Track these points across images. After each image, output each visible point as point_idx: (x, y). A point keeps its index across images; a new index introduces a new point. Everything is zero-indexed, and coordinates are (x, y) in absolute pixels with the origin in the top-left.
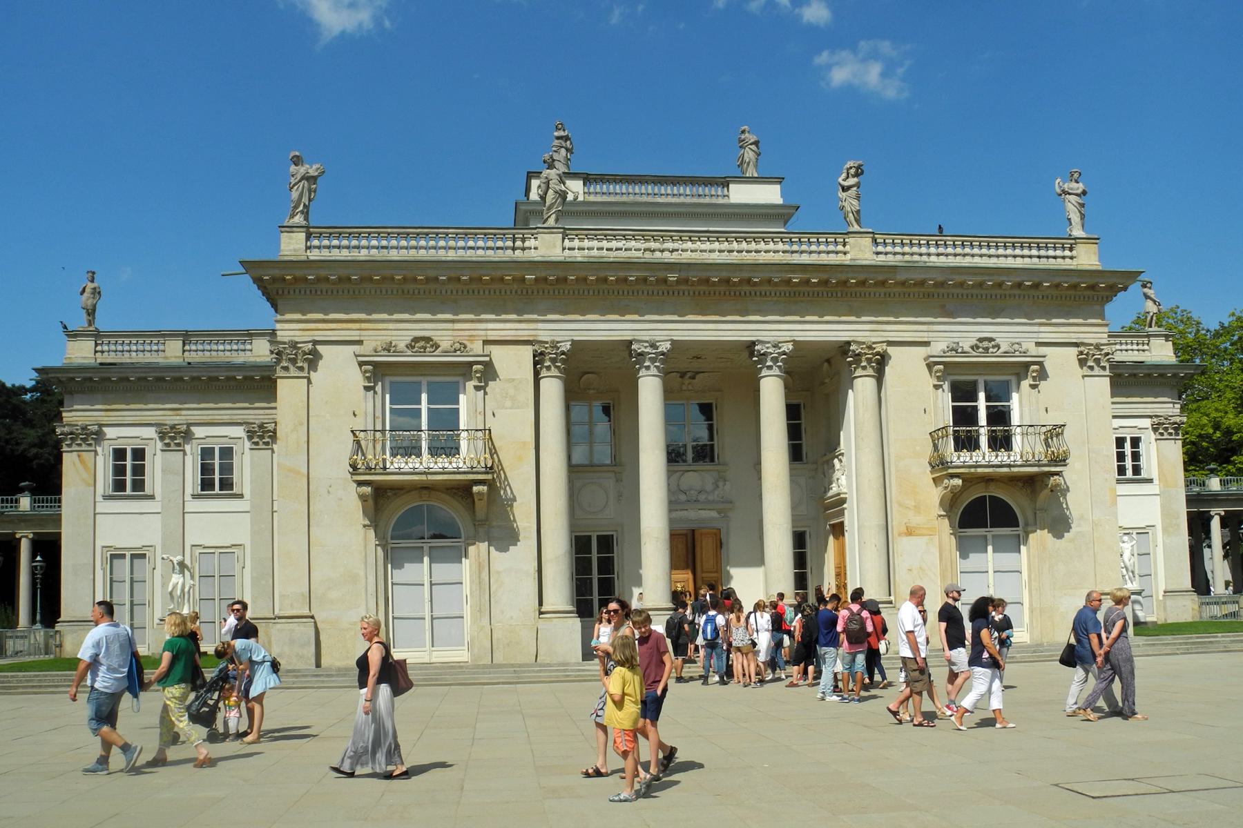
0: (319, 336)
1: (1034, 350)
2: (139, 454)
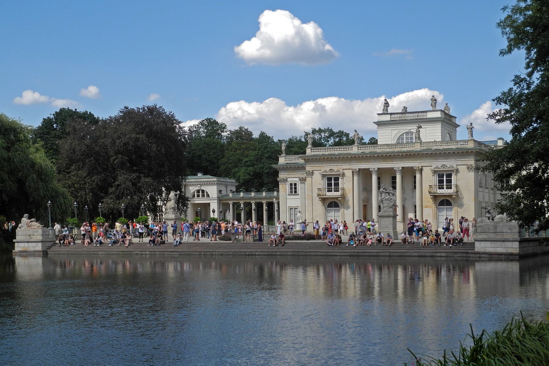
2: (295, 184)
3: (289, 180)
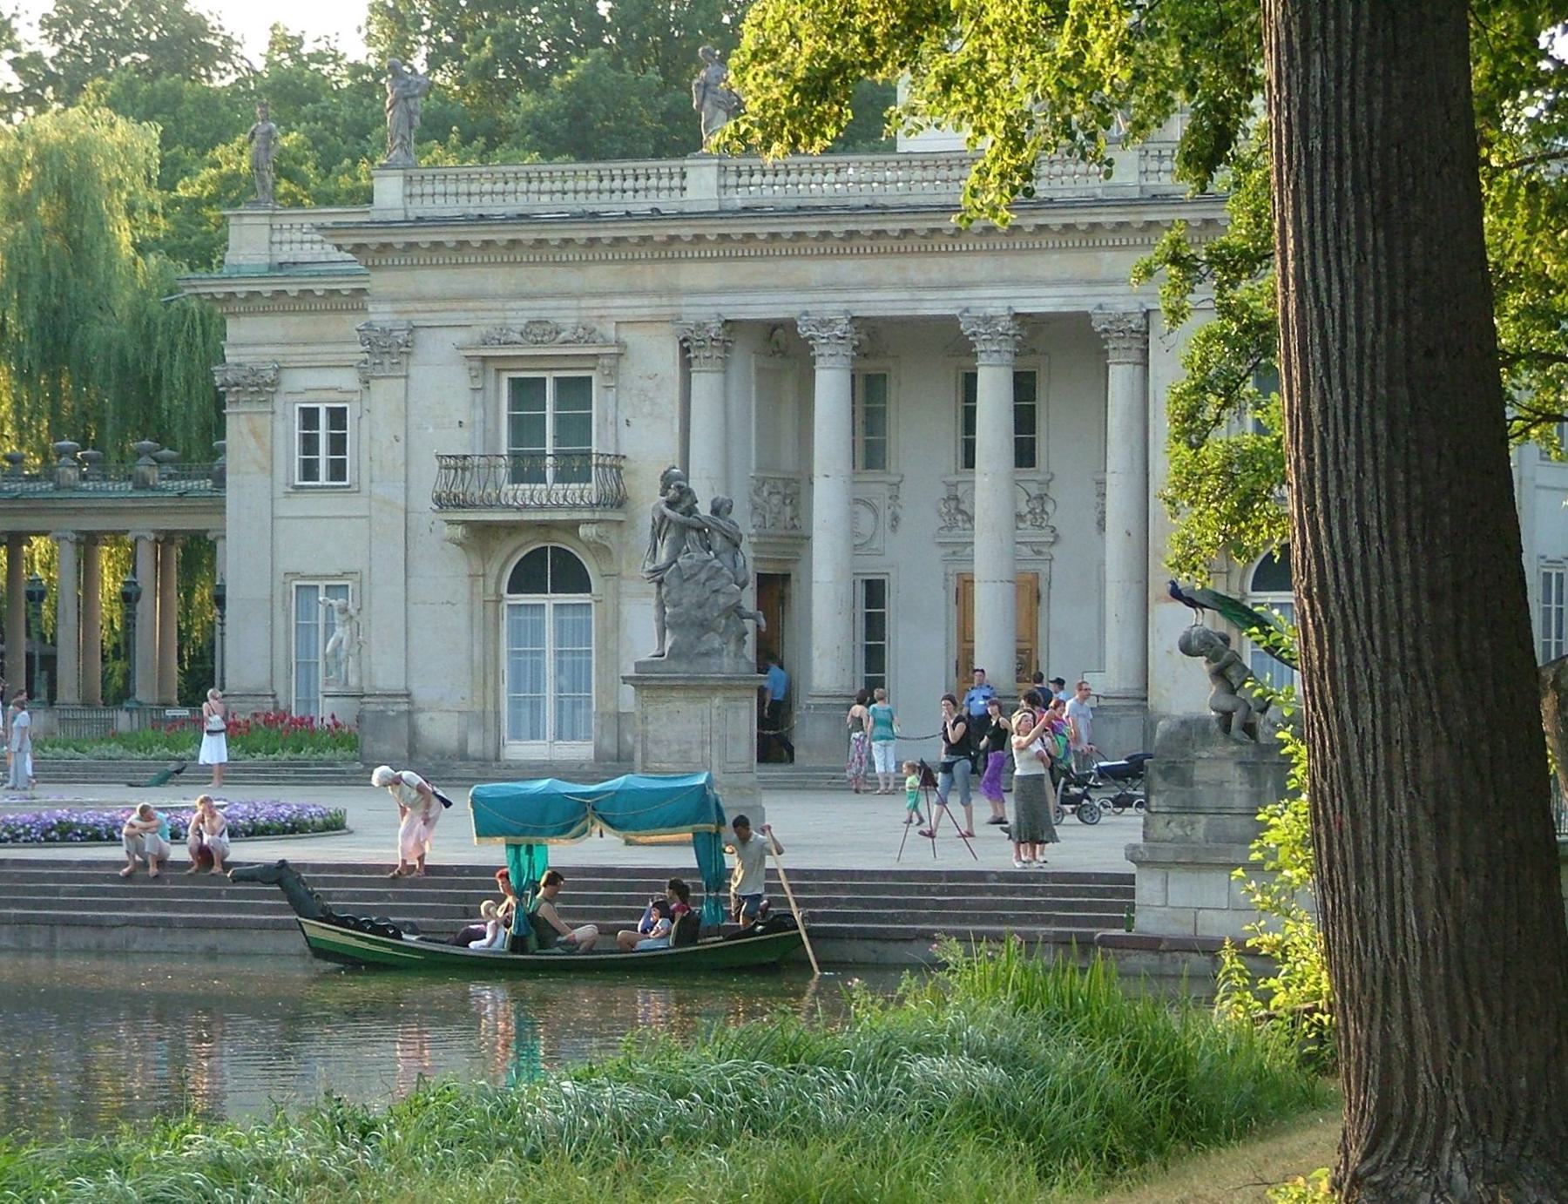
0: (419, 320)
3: (298, 380)
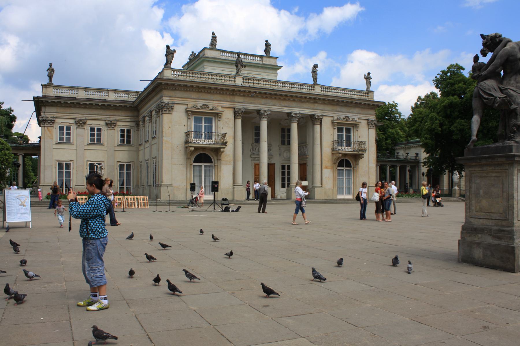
0: (176, 102)
1: (358, 121)
